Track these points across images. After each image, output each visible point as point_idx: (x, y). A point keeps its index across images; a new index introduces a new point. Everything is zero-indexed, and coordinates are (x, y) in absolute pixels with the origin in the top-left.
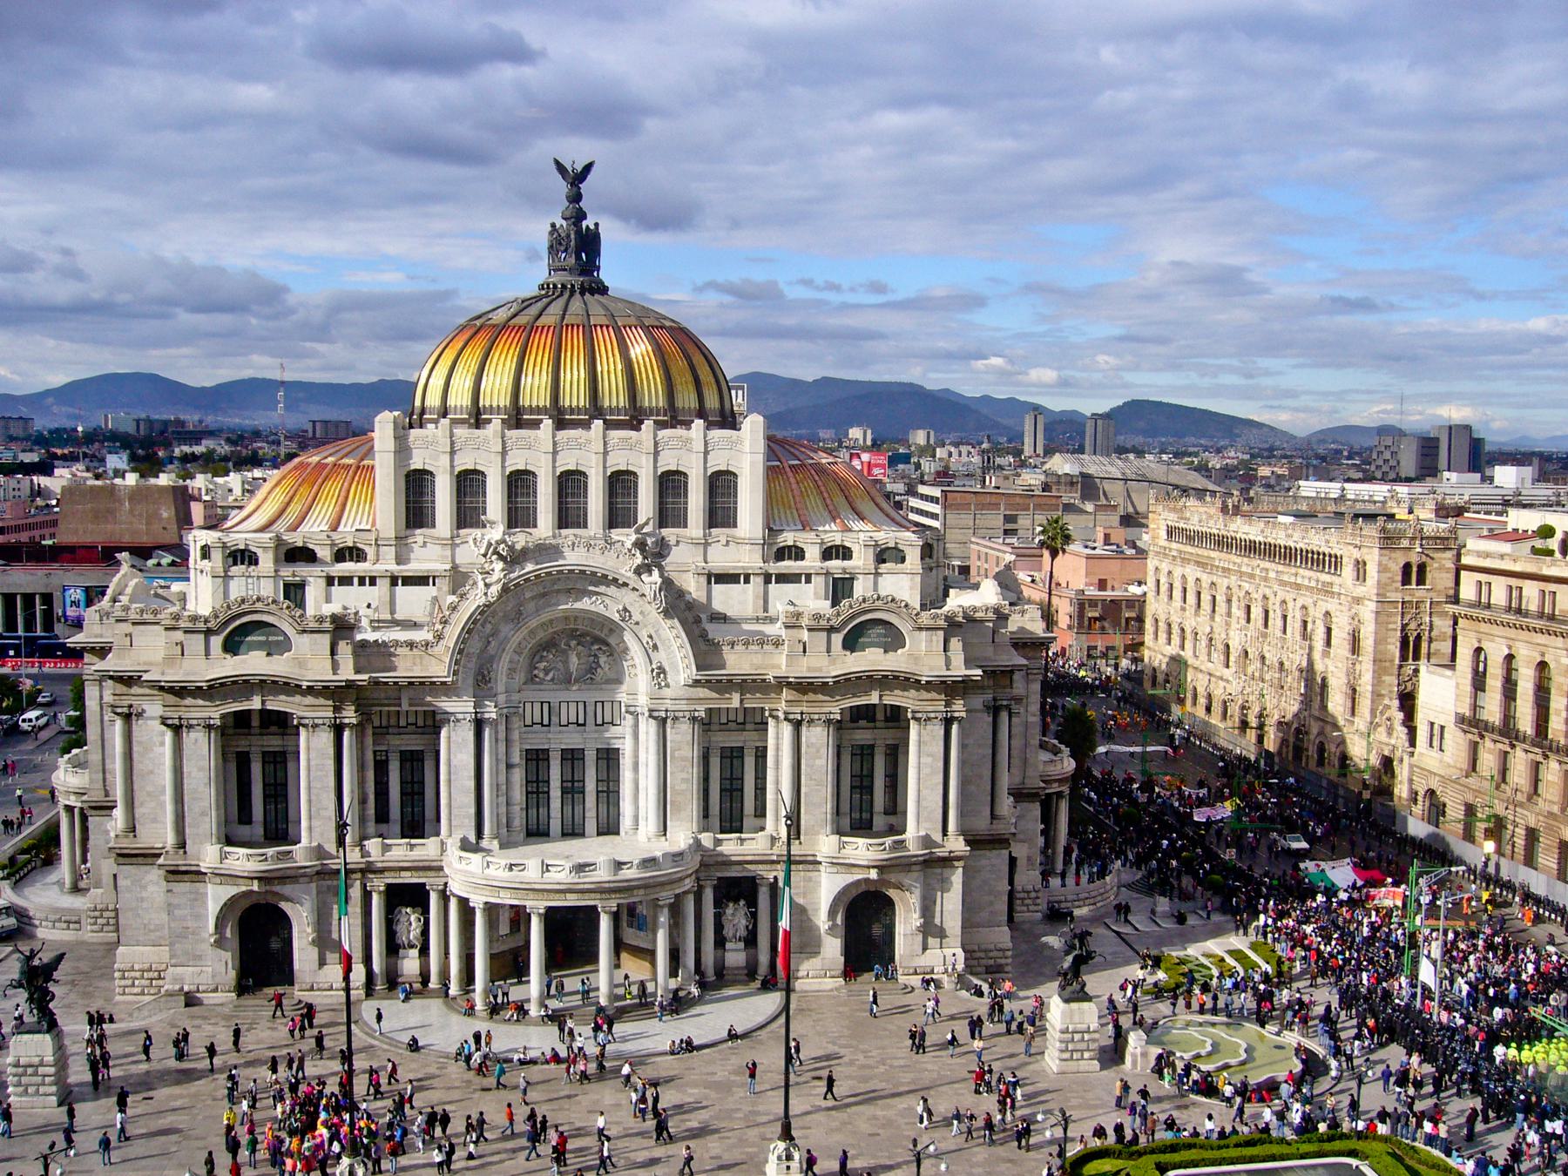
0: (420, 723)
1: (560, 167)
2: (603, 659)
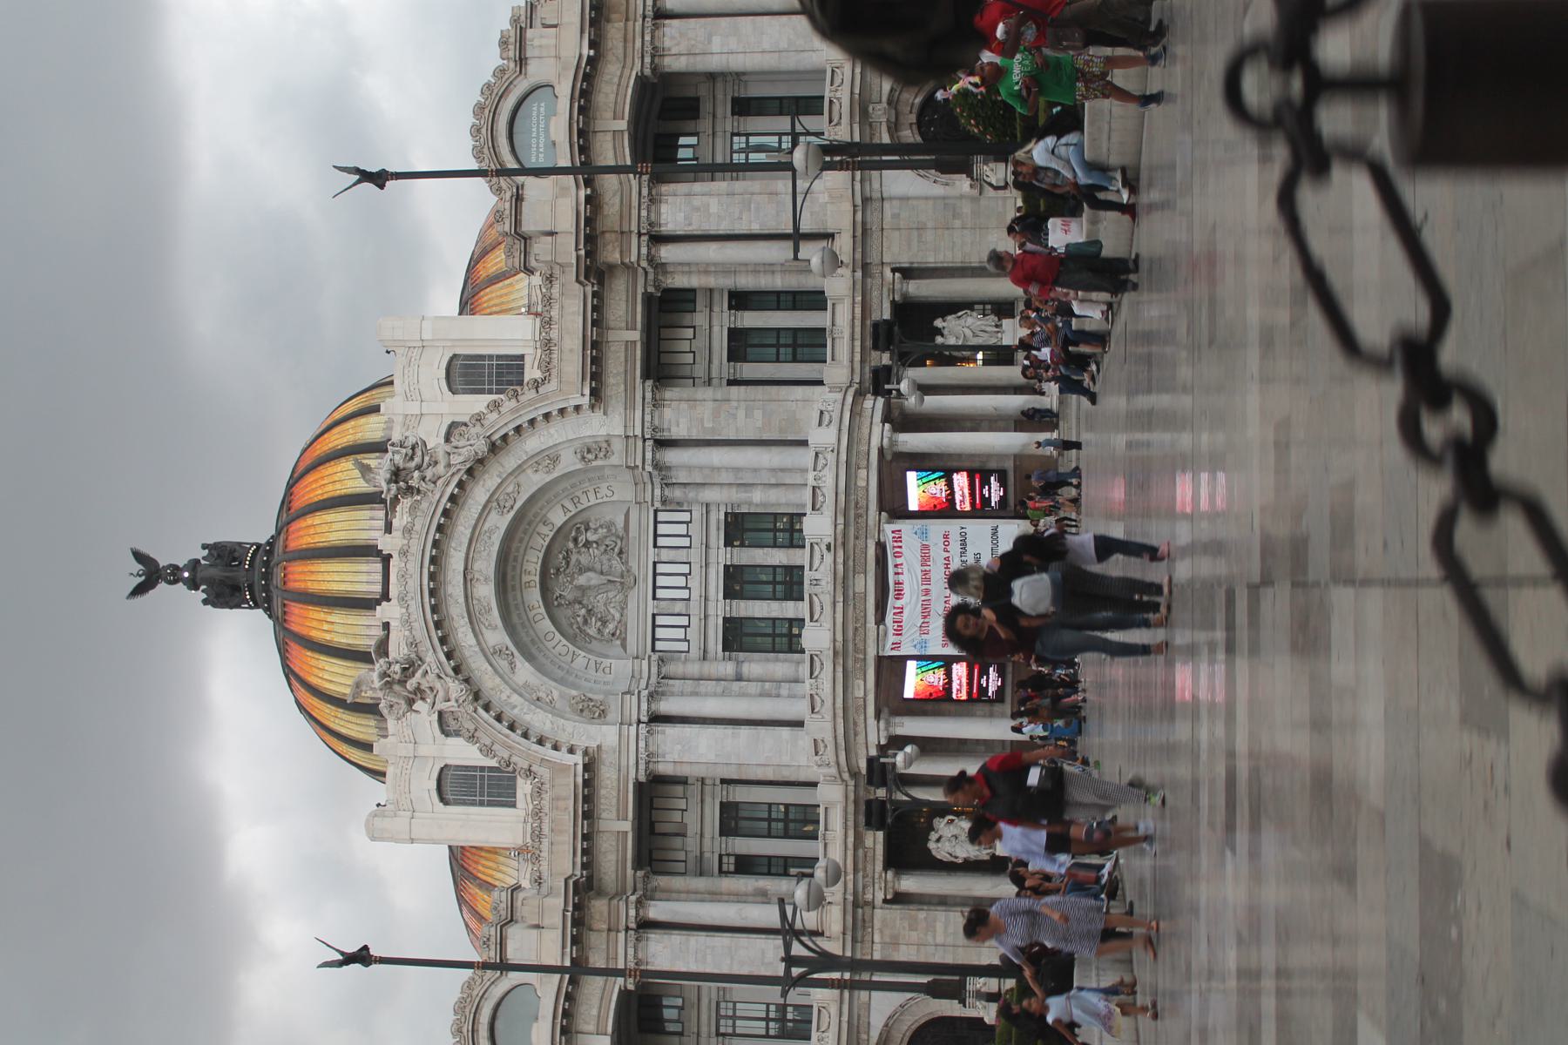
0: (682, 804)
1: (139, 590)
2: (591, 537)
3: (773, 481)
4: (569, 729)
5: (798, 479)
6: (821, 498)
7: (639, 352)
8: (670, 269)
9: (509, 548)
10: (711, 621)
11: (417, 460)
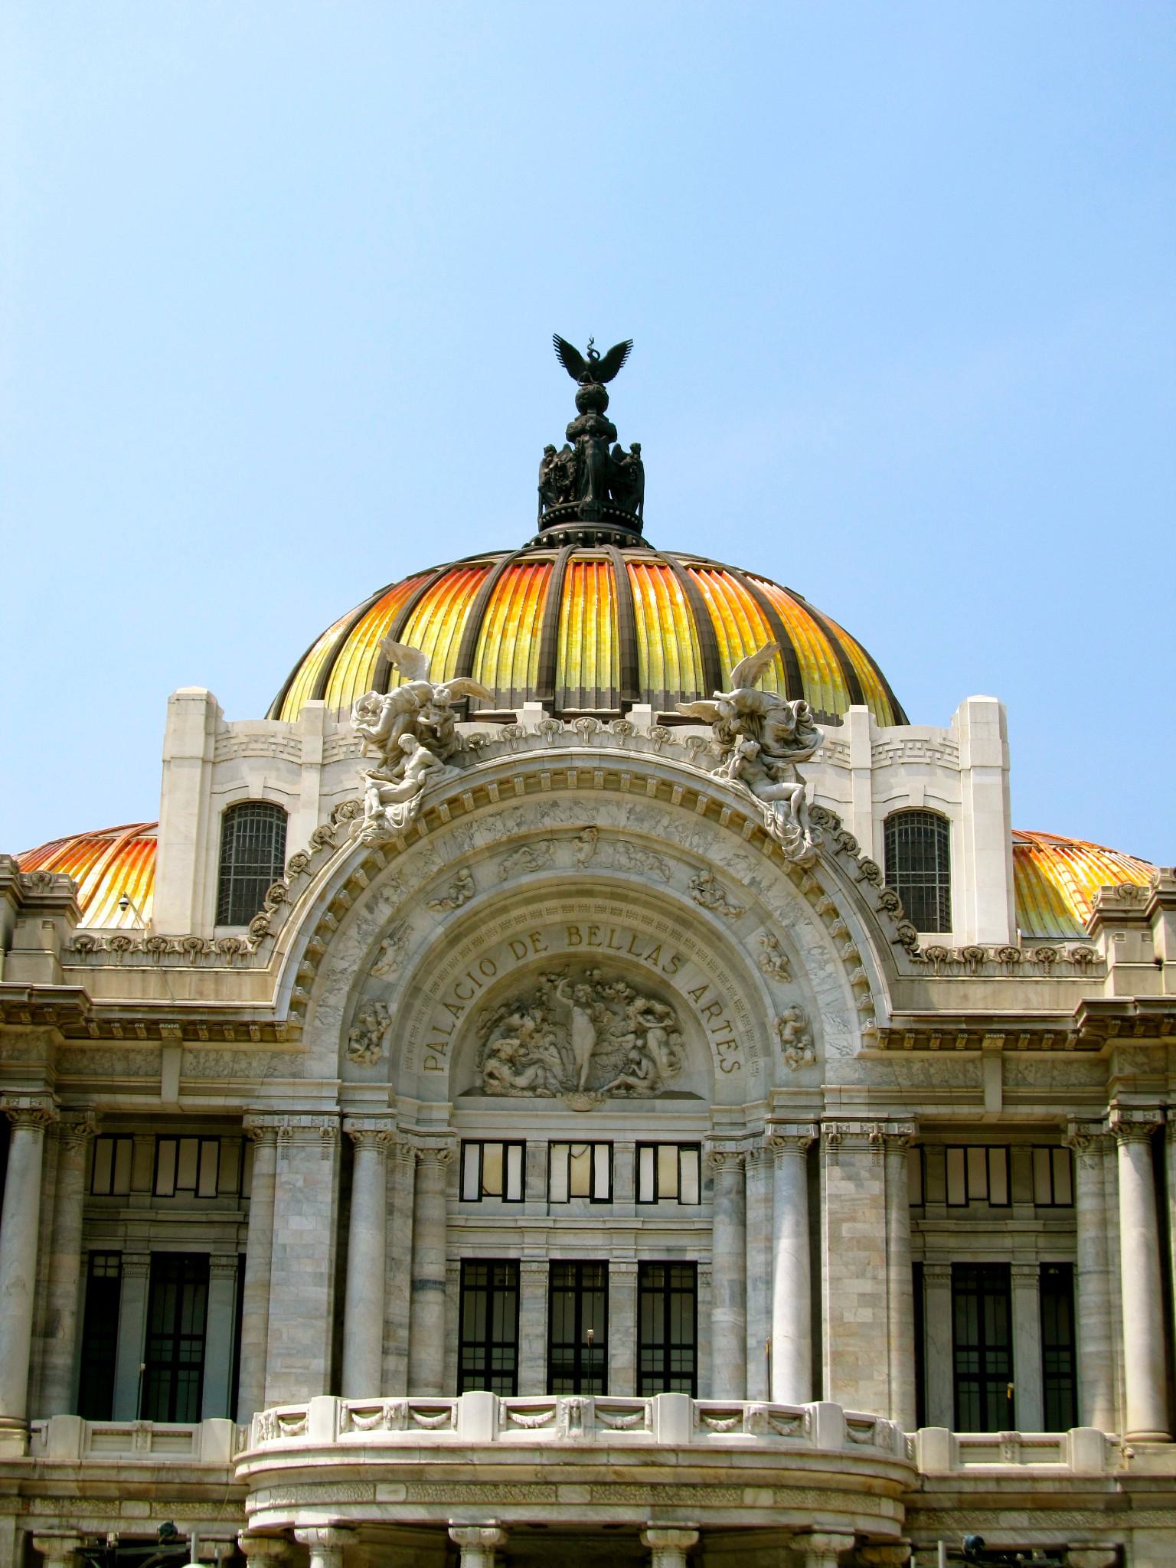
0: (207, 1188)
1: (567, 354)
2: (654, 1037)
3: (751, 1342)
4: (332, 1000)
5: (755, 1384)
6: (723, 1423)
7: (964, 1112)
8: (1107, 1160)
9: (634, 901)
10: (512, 1238)
11: (776, 748)
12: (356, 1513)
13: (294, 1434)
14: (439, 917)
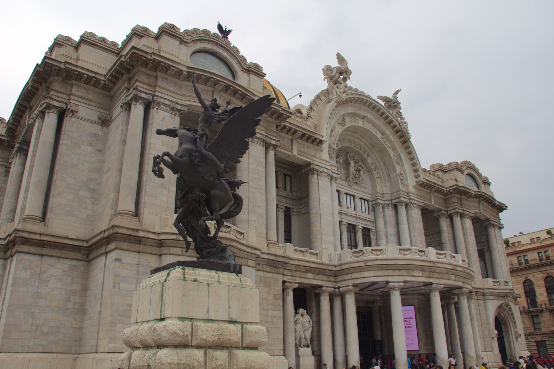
1: (220, 27)
2: (362, 172)
8: (448, 220)
9: (364, 138)
12: (409, 279)
13: (377, 255)
14: (341, 127)
